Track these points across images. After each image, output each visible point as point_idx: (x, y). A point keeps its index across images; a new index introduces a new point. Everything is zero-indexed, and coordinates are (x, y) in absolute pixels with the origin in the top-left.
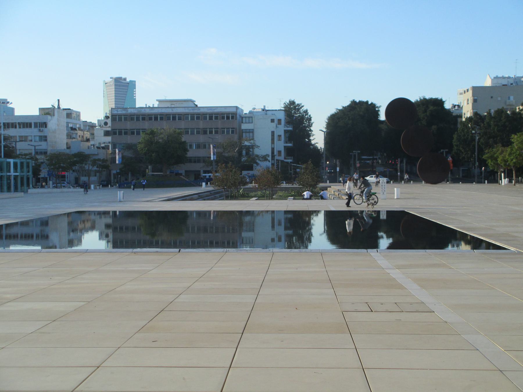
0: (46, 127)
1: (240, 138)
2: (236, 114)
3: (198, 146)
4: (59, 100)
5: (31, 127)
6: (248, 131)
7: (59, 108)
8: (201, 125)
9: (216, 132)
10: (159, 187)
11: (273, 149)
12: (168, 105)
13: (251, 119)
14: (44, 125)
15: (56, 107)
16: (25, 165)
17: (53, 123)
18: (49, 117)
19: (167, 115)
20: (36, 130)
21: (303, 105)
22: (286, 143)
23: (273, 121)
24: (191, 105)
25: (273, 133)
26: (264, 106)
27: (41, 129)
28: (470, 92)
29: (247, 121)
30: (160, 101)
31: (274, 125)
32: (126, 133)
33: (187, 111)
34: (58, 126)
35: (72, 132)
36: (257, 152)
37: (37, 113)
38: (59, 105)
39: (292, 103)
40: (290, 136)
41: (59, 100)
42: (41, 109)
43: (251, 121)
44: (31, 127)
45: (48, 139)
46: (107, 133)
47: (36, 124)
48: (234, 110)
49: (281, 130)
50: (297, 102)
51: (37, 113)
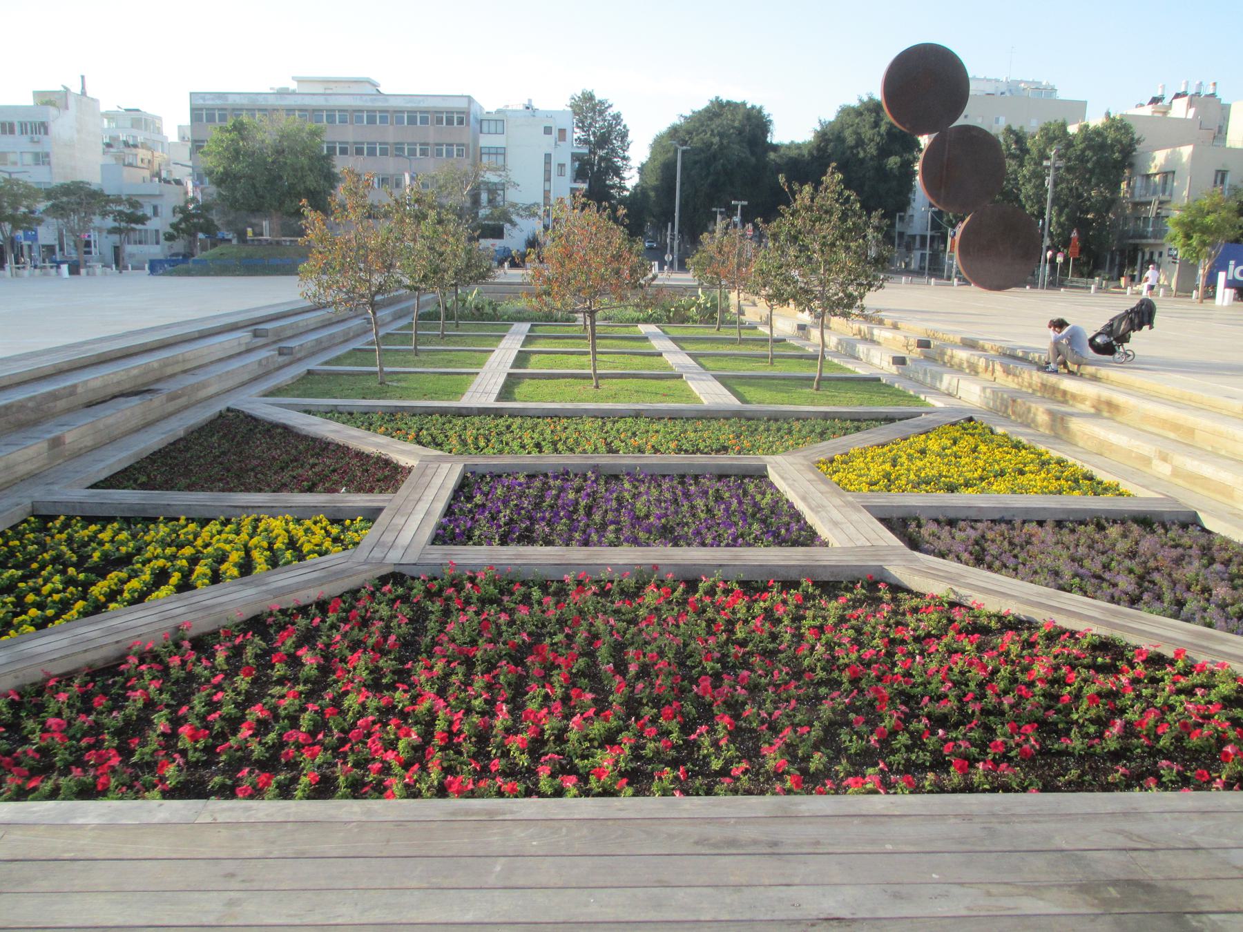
0: (46, 133)
1: (476, 164)
2: (468, 114)
4: (83, 77)
5: (12, 132)
6: (493, 151)
7: (84, 93)
8: (391, 135)
9: (424, 152)
10: (268, 274)
11: (547, 194)
12: (319, 89)
13: (500, 124)
14: (43, 128)
15: (76, 89)
17: (62, 126)
18: (53, 111)
19: (314, 110)
20: (25, 139)
21: (610, 102)
22: (575, 181)
23: (548, 131)
24: (369, 89)
25: (548, 157)
26: (530, 101)
27: (36, 137)
29: (493, 129)
30: (300, 81)
31: (550, 139)
34: (78, 131)
35: (127, 151)
36: (512, 196)
37: (29, 101)
38: (83, 88)
39: (589, 97)
40: (583, 169)
41: (83, 77)
42: (37, 94)
43: (499, 130)
44: (12, 132)
45: (53, 160)
47: (23, 125)
48: (463, 104)
49: (564, 155)
50: (598, 97)
51: (29, 101)
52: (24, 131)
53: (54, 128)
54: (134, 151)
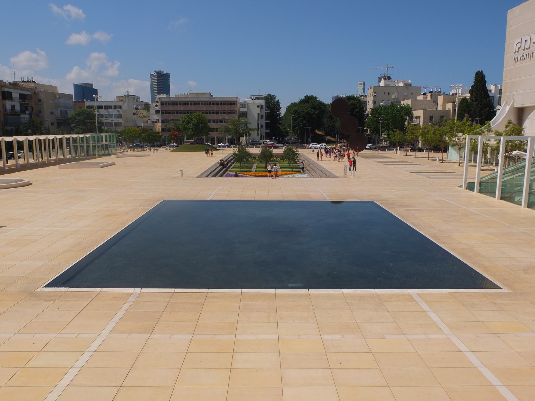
3: (213, 122)
5: (112, 108)
8: (215, 108)
11: (258, 124)
12: (195, 96)
16: (112, 136)
17: (125, 107)
23: (258, 106)
25: (258, 114)
28: (372, 90)
32: (170, 113)
33: (206, 100)
36: (249, 126)
40: (268, 116)
42: (118, 97)
44: (112, 108)
45: (123, 117)
46: (157, 112)
47: (115, 106)
52: (115, 108)
53: (123, 107)
54: (138, 111)
